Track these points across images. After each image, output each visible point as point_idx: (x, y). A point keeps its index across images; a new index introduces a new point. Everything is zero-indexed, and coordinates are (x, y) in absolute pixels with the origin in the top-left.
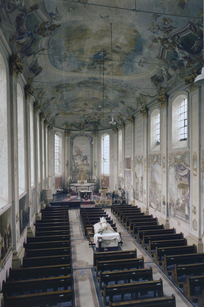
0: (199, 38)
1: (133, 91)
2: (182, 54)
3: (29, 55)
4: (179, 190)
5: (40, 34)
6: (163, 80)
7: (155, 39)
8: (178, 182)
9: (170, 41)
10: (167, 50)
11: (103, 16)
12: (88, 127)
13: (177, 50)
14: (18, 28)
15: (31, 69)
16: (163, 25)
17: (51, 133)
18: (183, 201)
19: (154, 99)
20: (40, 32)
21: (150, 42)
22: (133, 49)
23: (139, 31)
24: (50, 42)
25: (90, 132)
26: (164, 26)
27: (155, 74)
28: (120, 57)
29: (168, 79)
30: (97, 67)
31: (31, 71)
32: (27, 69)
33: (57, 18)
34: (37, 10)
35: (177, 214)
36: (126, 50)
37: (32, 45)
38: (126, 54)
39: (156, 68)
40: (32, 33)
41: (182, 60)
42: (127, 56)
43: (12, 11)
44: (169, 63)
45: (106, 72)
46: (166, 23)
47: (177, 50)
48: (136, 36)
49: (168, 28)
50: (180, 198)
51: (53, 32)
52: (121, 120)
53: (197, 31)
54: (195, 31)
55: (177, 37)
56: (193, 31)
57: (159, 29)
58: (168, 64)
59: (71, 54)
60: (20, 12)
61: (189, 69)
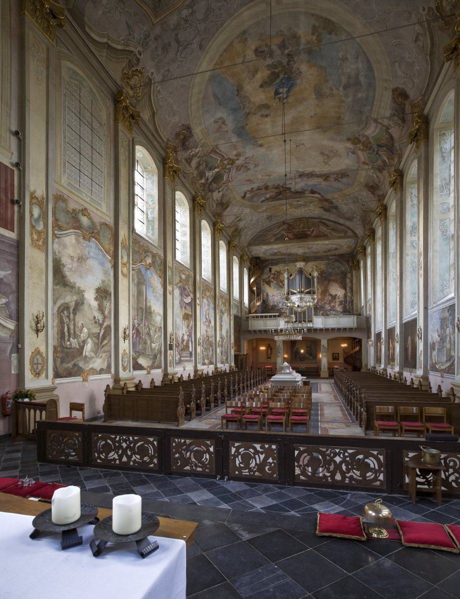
3: (392, 138)
4: (183, 321)
13: (217, 170)
18: (188, 336)
20: (369, 145)
21: (241, 150)
22: (247, 127)
27: (195, 135)
28: (252, 102)
30: (279, 52)
34: (364, 161)
36: (254, 120)
38: (249, 114)
39: (202, 139)
42: (245, 112)
45: (252, 45)
47: (217, 170)
50: (184, 333)
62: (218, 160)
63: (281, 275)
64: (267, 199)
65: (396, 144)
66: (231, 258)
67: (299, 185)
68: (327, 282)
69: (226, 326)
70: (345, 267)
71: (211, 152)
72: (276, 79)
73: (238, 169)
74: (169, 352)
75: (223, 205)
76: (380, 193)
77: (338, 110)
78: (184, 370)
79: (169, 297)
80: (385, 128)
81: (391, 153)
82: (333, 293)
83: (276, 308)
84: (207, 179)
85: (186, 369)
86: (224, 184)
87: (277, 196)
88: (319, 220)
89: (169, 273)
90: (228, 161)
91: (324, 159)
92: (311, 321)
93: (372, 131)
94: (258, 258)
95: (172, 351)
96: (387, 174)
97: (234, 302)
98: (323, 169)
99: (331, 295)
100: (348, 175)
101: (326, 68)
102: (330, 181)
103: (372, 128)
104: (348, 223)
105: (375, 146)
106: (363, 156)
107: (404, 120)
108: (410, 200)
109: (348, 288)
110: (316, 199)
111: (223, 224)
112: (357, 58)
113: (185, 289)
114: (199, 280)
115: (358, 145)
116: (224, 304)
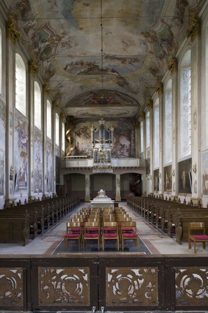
3: (172, 34)
4: (21, 158)
7: (65, 35)
8: (21, 149)
11: (110, 34)
13: (47, 43)
20: (156, 39)
22: (73, 12)
27: (32, 9)
35: (21, 186)
37: (165, 38)
44: (38, 31)
46: (69, 46)
47: (47, 43)
49: (65, 45)
50: (22, 167)
56: (53, 54)
63: (88, 130)
64: (81, 73)
65: (174, 40)
66: (54, 114)
67: (106, 64)
68: (119, 136)
69: (50, 164)
70: (130, 126)
71: (44, 27)
73: (63, 45)
74: (9, 181)
75: (51, 73)
76: (159, 75)
77: (138, 9)
78: (21, 196)
79: (10, 137)
80: (168, 27)
81: (170, 46)
82: (123, 144)
83: (84, 153)
84: (40, 50)
85: (23, 195)
86: (52, 56)
87: (88, 71)
88: (115, 92)
89: (10, 117)
90: (56, 37)
91: (124, 47)
92: (109, 162)
93: (159, 29)
94: (72, 117)
95: (12, 181)
96: (166, 61)
97: (56, 147)
98: (122, 54)
99: (121, 145)
100: (139, 60)
102: (126, 64)
104: (134, 96)
105: (160, 40)
106: (150, 46)
107: (182, 22)
108: (183, 78)
109: (132, 141)
110: (115, 77)
111: (49, 87)
113: (22, 132)
114: (32, 127)
115: (148, 38)
116: (49, 147)
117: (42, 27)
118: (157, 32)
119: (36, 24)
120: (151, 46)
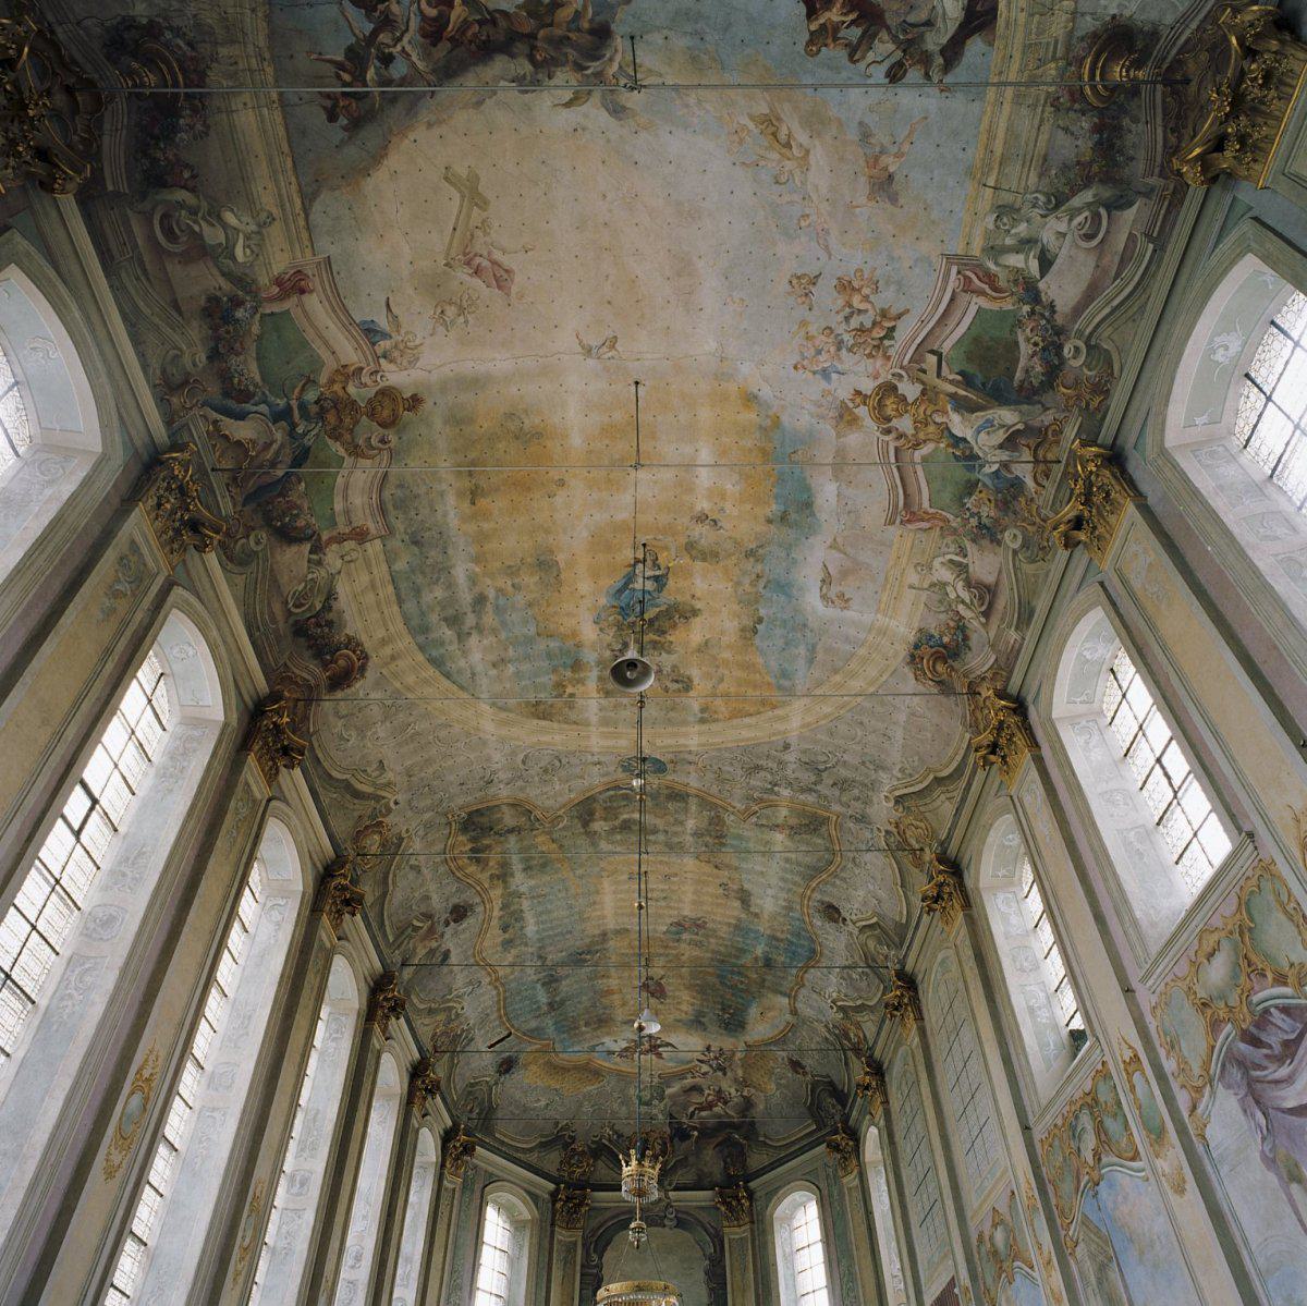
0: (1026, 308)
1: (859, 798)
2: (988, 433)
3: (288, 535)
5: (336, 439)
6: (966, 638)
9: (910, 390)
10: (918, 455)
11: (594, 344)
12: (692, 1159)
13: (959, 425)
14: (214, 355)
15: (300, 630)
16: (847, 319)
17: (465, 1186)
19: (963, 783)
20: (331, 418)
21: (827, 429)
23: (760, 394)
24: (387, 494)
25: (703, 1197)
26: (855, 322)
27: (916, 625)
29: (987, 614)
31: (302, 640)
32: (272, 614)
33: (396, 354)
34: (305, 298)
38: (750, 554)
39: (911, 587)
40: (289, 408)
41: (1005, 465)
42: (759, 567)
43: (187, 258)
44: (954, 525)
46: (856, 301)
47: (959, 425)
48: (761, 427)
49: (874, 323)
51: (392, 437)
52: (857, 1051)
53: (1002, 283)
54: (996, 290)
55: (933, 359)
56: (982, 293)
57: (840, 345)
58: (955, 532)
59: (500, 583)
60: (226, 286)
61: (1051, 487)
62: (925, 459)
72: (657, 617)
77: (486, 526)
90: (895, 423)
91: (484, 226)
101: (539, 635)
103: (358, 500)
112: (473, 674)
117: (928, 520)
118: (348, 461)
119: (940, 559)
120: (326, 344)
